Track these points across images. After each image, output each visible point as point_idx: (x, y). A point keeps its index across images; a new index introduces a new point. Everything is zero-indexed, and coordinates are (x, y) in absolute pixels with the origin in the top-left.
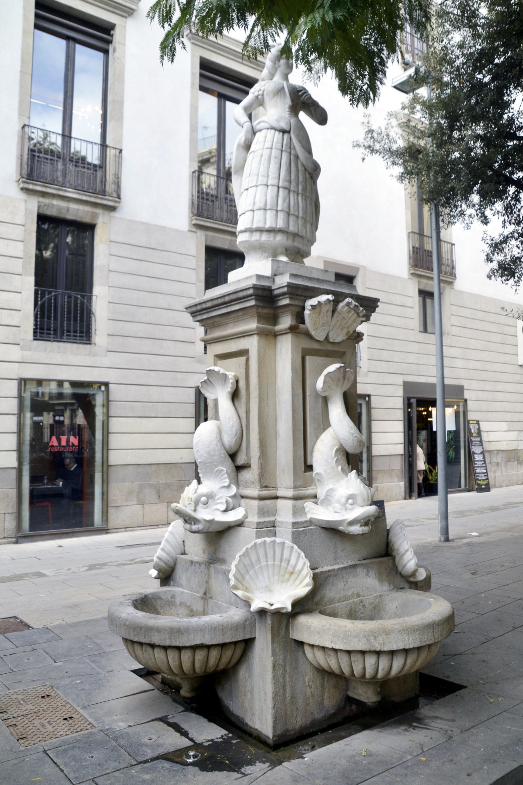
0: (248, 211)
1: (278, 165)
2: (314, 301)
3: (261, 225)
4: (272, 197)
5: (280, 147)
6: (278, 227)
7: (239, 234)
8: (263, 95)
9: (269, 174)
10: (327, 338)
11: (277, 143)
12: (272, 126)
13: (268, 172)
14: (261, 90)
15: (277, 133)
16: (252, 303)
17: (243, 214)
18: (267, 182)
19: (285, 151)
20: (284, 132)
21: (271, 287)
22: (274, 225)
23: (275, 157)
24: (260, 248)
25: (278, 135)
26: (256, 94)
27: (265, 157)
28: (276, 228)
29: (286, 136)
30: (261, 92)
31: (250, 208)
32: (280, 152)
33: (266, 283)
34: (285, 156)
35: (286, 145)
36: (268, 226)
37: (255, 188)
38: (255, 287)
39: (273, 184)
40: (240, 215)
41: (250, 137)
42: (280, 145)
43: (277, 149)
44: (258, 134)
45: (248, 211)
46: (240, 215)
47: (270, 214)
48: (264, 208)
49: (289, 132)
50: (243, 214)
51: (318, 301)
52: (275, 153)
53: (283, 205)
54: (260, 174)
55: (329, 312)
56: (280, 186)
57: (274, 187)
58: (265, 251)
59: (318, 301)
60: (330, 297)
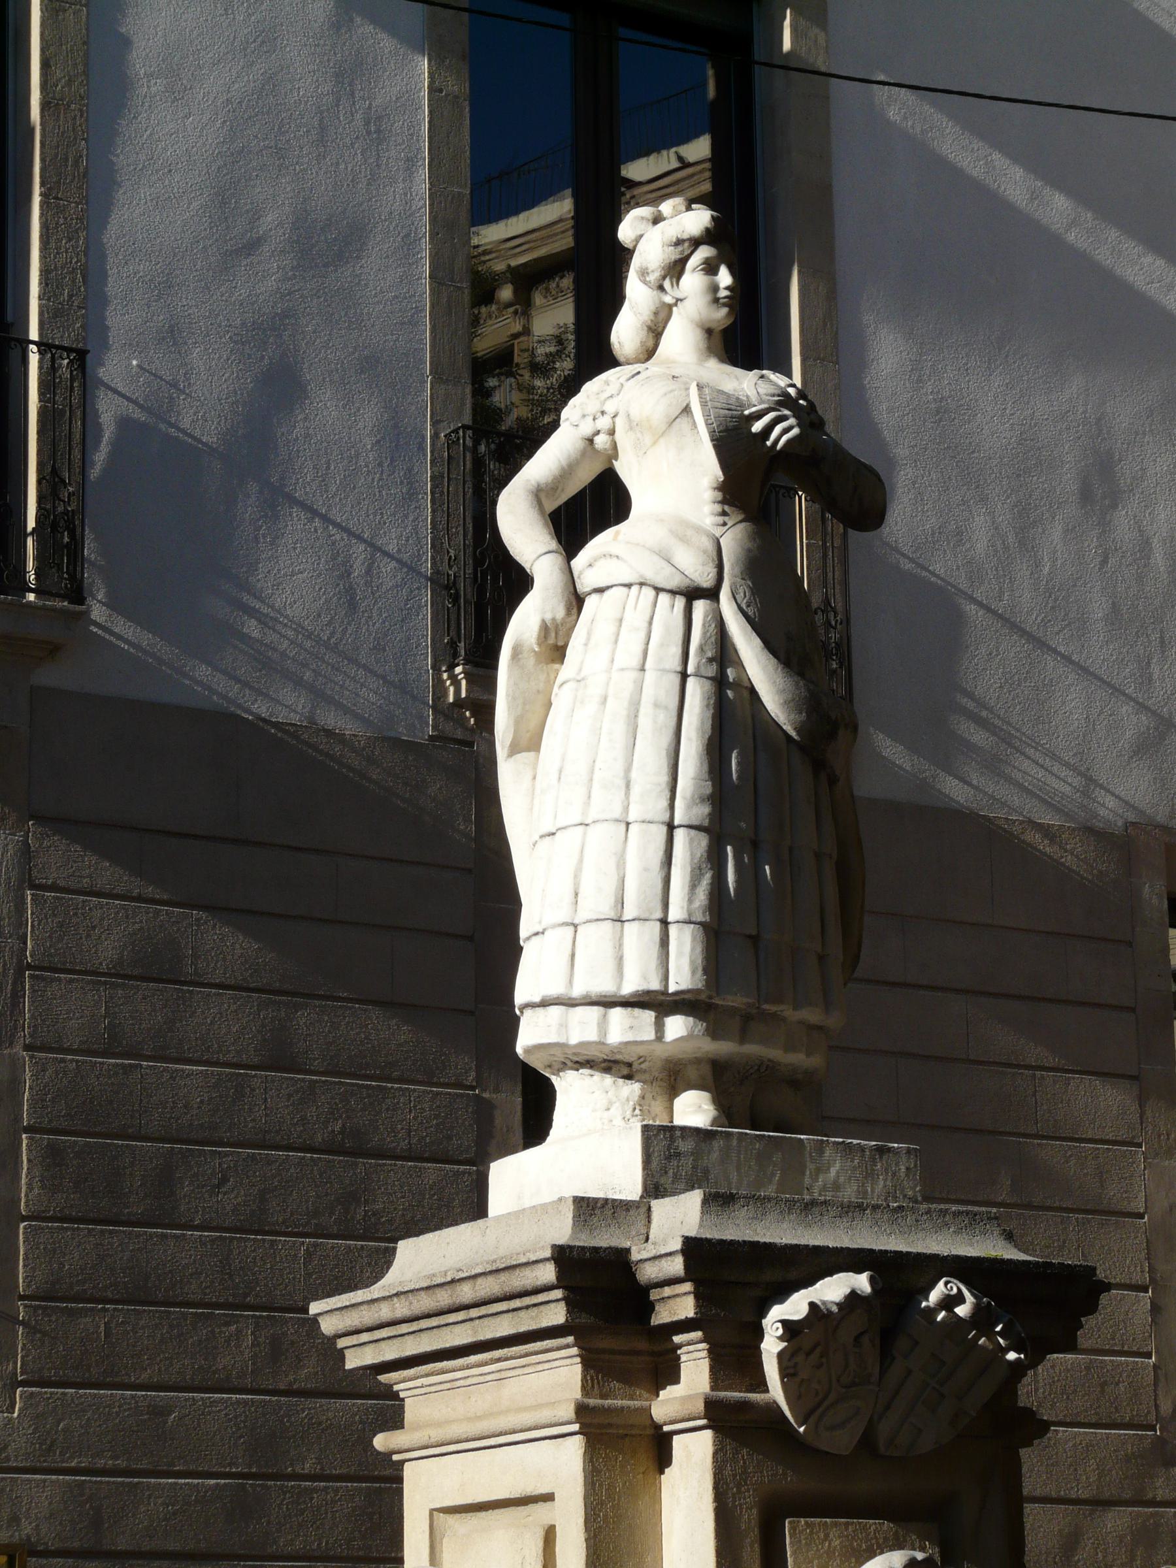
0: (554, 926)
1: (666, 738)
2: (795, 1306)
3: (604, 985)
4: (646, 870)
5: (675, 663)
6: (672, 988)
7: (522, 1012)
8: (612, 432)
9: (634, 775)
10: (867, 1443)
11: (662, 645)
12: (641, 576)
13: (628, 770)
14: (603, 413)
15: (664, 598)
16: (557, 1315)
17: (537, 934)
18: (626, 809)
19: (697, 675)
20: (692, 594)
21: (628, 1251)
22: (655, 985)
23: (656, 705)
24: (614, 1064)
25: (670, 611)
26: (587, 428)
27: (618, 707)
28: (664, 992)
29: (700, 607)
30: (604, 423)
31: (564, 915)
32: (677, 680)
33: (606, 1238)
34: (696, 692)
35: (701, 649)
36: (629, 988)
37: (581, 828)
38: (562, 1256)
39: (649, 817)
40: (528, 938)
41: (560, 613)
42: (676, 650)
43: (664, 671)
44: (590, 603)
45: (554, 926)
46: (528, 938)
47: (639, 941)
48: (612, 915)
49: (712, 594)
50: (537, 934)
51: (812, 1305)
52: (659, 686)
53: (690, 901)
54: (597, 775)
55: (865, 1340)
56: (676, 823)
57: (654, 827)
58: (629, 1077)
59: (812, 1305)
60: (862, 1282)
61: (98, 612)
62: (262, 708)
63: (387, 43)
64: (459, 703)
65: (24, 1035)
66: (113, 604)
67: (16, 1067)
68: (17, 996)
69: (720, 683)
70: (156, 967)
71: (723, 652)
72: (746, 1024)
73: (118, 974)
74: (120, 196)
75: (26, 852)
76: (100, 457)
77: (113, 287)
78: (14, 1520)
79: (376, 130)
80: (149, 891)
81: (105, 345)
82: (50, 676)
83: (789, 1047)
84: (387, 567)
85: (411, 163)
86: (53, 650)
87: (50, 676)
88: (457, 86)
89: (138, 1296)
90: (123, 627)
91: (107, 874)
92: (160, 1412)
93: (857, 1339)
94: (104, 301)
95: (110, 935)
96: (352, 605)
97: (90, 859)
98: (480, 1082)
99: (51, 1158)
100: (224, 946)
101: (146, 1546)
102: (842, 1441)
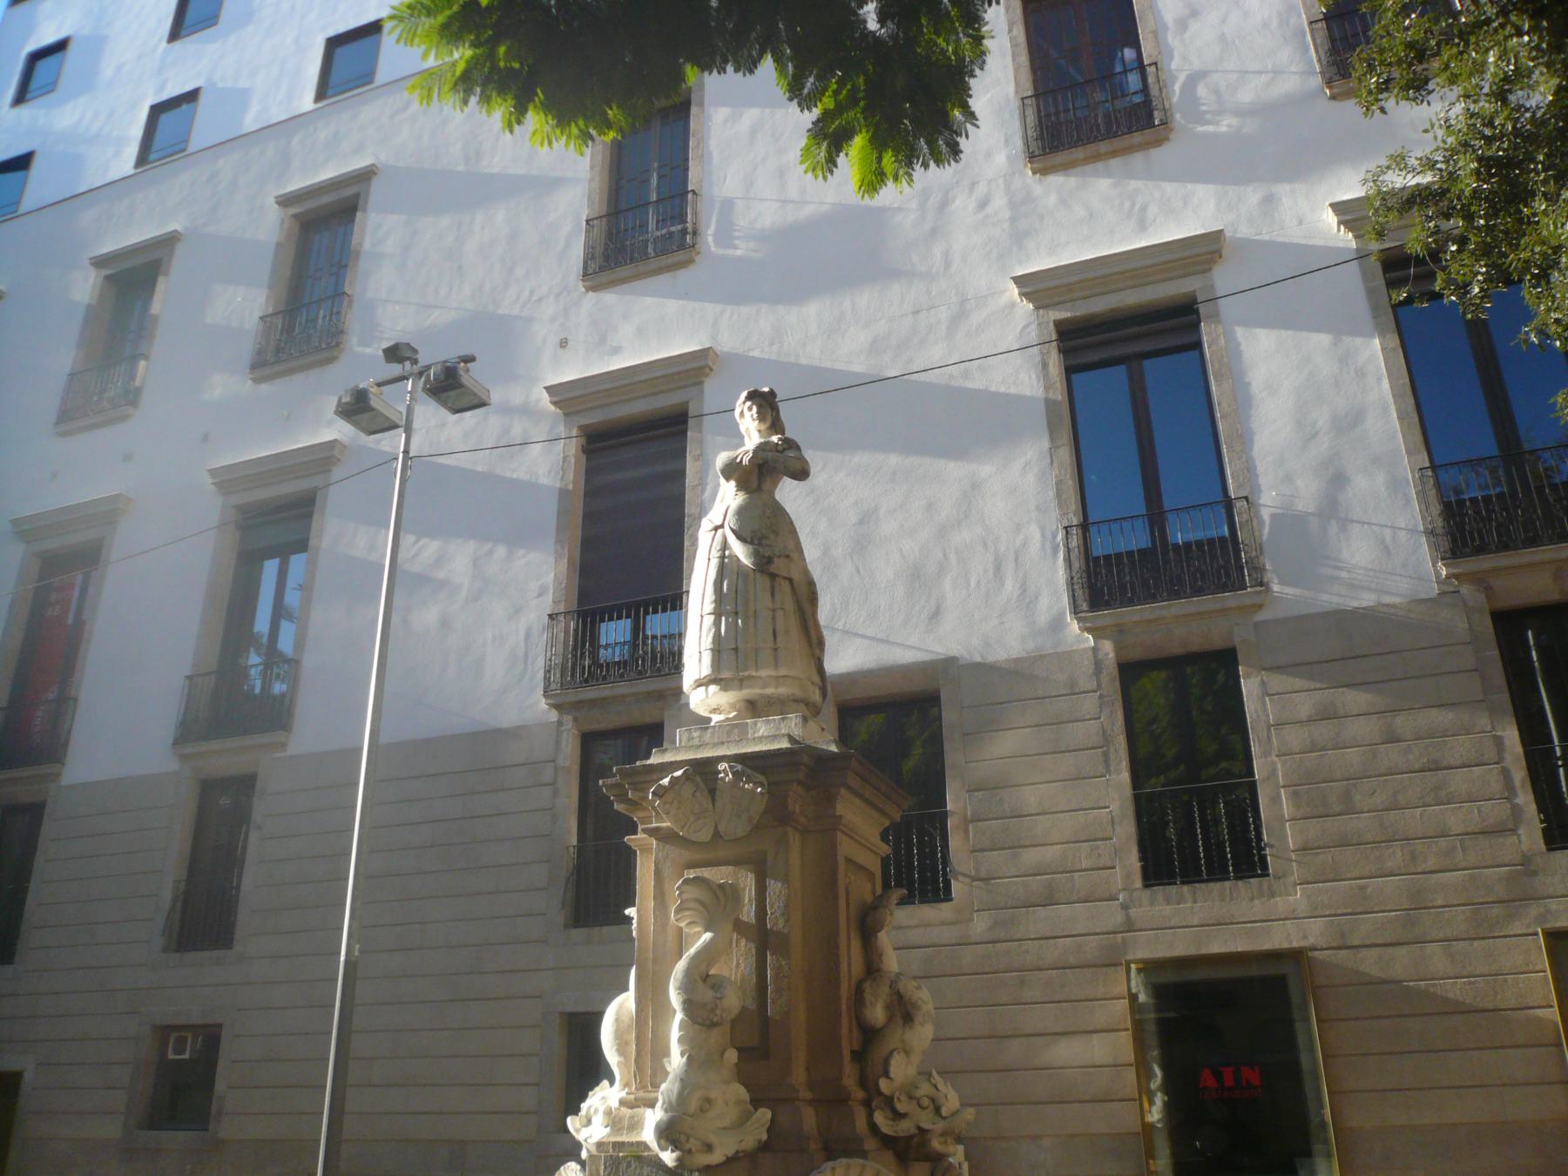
10: (717, 835)
49: (722, 526)
61: (1276, 588)
62: (1355, 604)
63: (1358, 340)
64: (1448, 577)
65: (1275, 752)
66: (1282, 582)
67: (1273, 763)
68: (1269, 737)
69: (723, 557)
70: (1327, 714)
71: (725, 545)
72: (741, 682)
73: (1310, 720)
74: (1256, 438)
75: (1263, 683)
76: (1266, 531)
77: (1260, 469)
78: (1305, 937)
79: (1361, 374)
80: (1318, 685)
81: (1260, 491)
82: (1262, 616)
83: (764, 686)
84: (1402, 535)
85: (1379, 380)
86: (1260, 606)
87: (1262, 616)
88: (1394, 341)
89: (1344, 843)
90: (1288, 590)
91: (1298, 683)
92: (1362, 888)
93: (693, 795)
94: (1257, 476)
95: (1304, 706)
96: (1389, 553)
97: (1291, 679)
98: (1493, 728)
99: (1295, 796)
100: (1355, 699)
101: (1368, 942)
102: (704, 835)
